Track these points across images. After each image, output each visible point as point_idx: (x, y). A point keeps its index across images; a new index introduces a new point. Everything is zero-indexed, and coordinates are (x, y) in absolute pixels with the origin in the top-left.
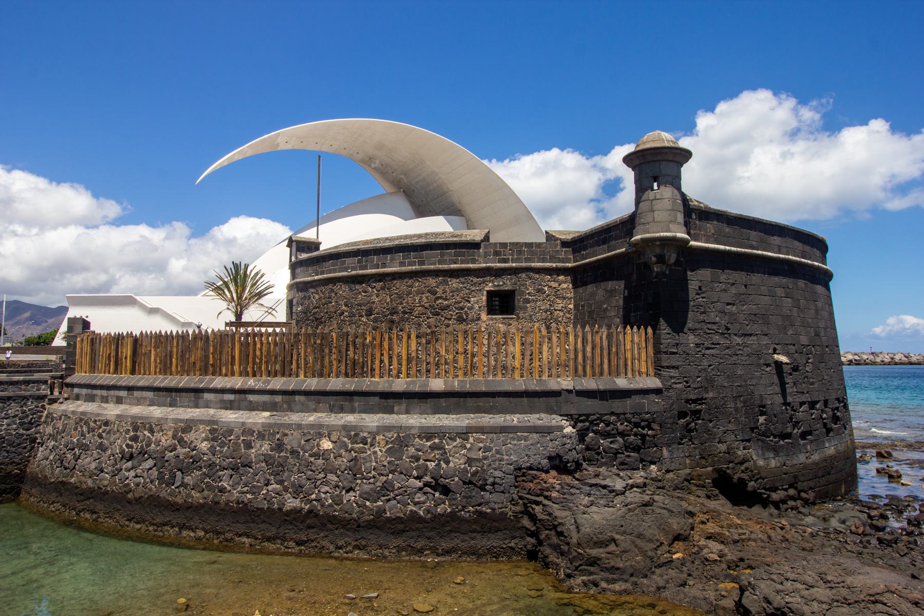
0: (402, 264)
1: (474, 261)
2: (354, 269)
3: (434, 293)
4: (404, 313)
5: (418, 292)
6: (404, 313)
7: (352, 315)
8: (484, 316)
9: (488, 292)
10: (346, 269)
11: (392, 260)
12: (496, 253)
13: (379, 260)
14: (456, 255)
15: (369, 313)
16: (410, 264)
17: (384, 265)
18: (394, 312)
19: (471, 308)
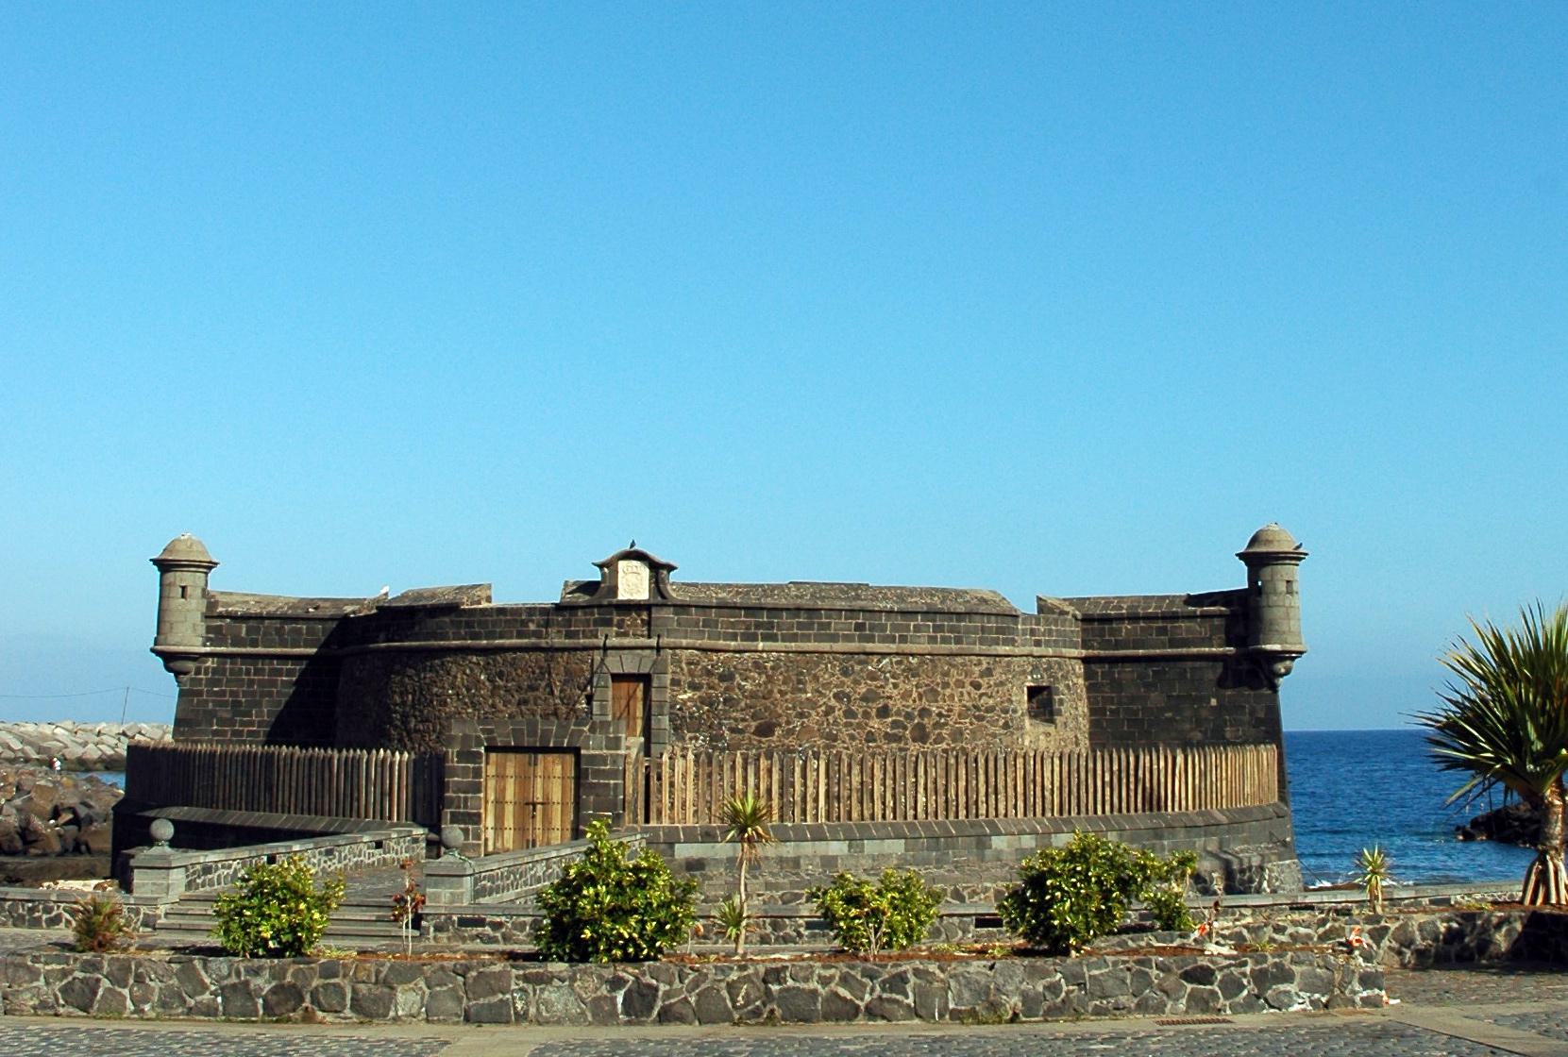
0: (932, 640)
1: (1012, 642)
2: (848, 638)
3: (977, 686)
4: (940, 715)
5: (960, 684)
6: (940, 715)
7: (849, 714)
8: (1027, 722)
9: (1030, 688)
10: (834, 638)
11: (917, 629)
12: (1033, 632)
13: (895, 628)
14: (1000, 630)
15: (884, 712)
16: (945, 640)
17: (903, 639)
18: (924, 712)
19: (1015, 711)
